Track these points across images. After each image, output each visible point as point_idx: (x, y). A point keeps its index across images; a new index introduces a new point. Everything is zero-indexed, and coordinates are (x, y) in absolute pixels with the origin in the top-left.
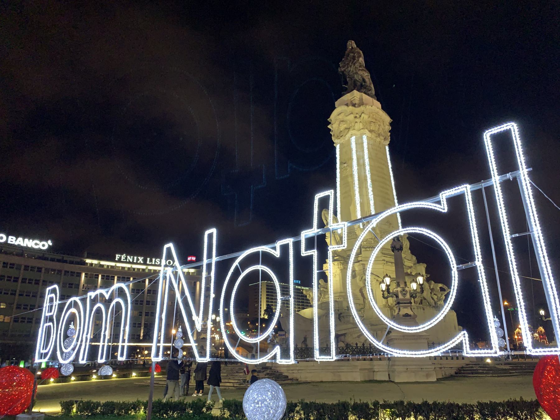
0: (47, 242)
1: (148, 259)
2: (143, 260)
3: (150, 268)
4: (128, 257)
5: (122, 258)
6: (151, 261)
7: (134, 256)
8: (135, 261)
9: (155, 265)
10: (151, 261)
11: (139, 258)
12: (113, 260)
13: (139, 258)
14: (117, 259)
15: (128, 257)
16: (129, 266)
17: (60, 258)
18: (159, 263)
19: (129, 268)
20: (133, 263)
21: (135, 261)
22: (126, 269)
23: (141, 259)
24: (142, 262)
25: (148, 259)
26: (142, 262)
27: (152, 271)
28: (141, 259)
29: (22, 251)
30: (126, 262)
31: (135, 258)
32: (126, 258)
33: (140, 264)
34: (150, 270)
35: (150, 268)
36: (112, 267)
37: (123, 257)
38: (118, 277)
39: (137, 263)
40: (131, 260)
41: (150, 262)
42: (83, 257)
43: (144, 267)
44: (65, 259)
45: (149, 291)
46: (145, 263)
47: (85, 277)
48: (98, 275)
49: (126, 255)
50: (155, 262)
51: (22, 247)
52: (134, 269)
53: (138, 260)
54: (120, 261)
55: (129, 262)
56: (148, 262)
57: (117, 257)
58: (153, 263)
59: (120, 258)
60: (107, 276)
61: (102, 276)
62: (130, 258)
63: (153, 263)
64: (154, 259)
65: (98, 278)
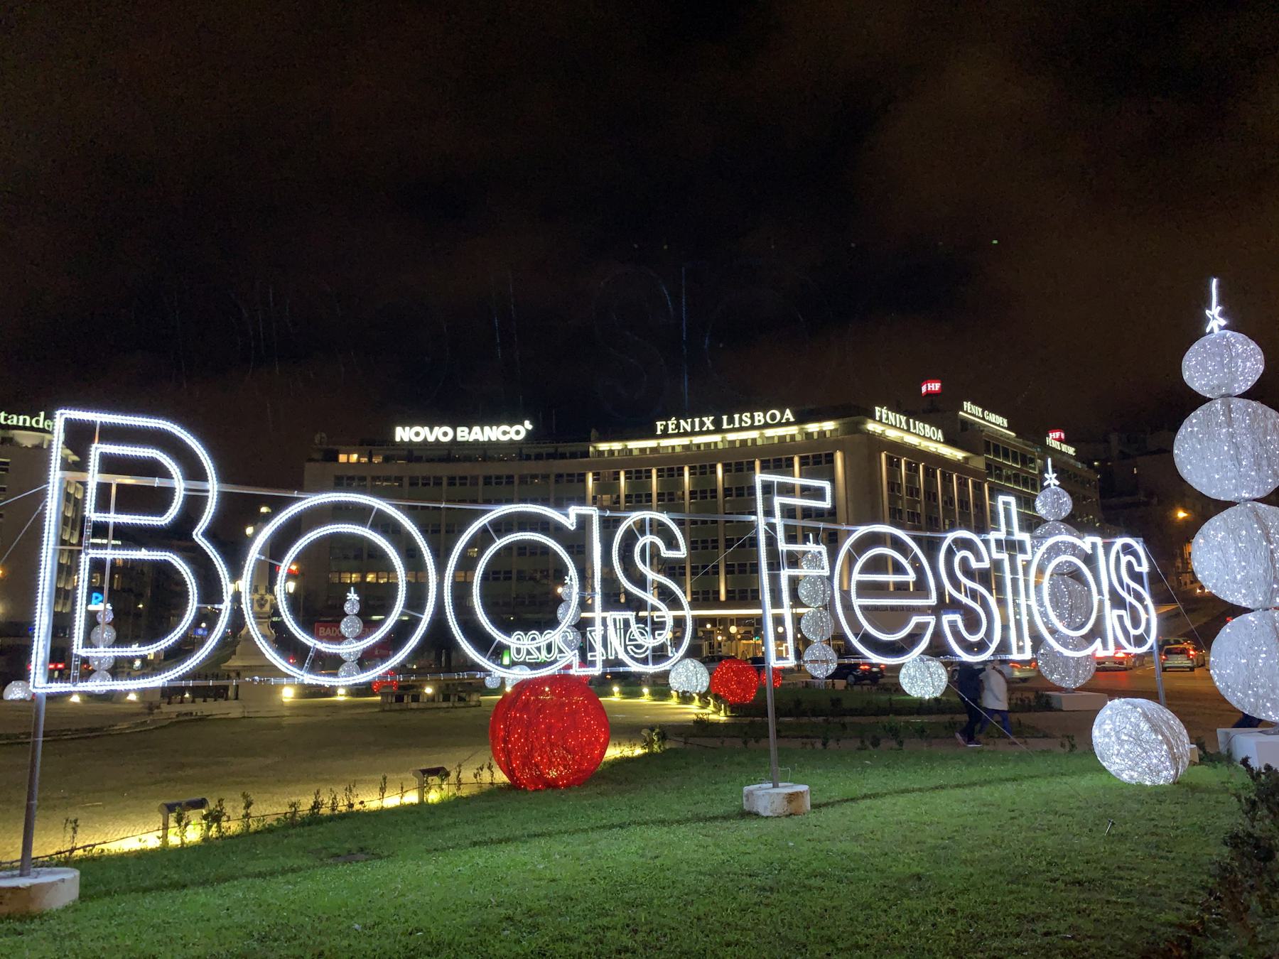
0: (523, 424)
1: (725, 418)
2: (713, 423)
3: (731, 437)
4: (682, 422)
5: (671, 427)
6: (731, 421)
7: (693, 417)
8: (697, 429)
9: (741, 429)
10: (731, 421)
11: (705, 419)
12: (652, 435)
13: (705, 419)
14: (659, 432)
15: (682, 422)
16: (685, 441)
17: (552, 450)
18: (749, 422)
19: (684, 446)
20: (693, 433)
21: (697, 429)
22: (636, 453)
23: (708, 421)
24: (712, 428)
25: (725, 418)
26: (712, 428)
27: (738, 445)
28: (708, 421)
29: (486, 451)
30: (679, 435)
31: (697, 420)
32: (678, 426)
33: (708, 432)
34: (734, 442)
35: (731, 437)
36: (653, 450)
37: (672, 424)
38: (658, 471)
39: (701, 433)
40: (689, 429)
41: (729, 423)
42: (588, 440)
43: (716, 438)
44: (560, 450)
45: (727, 491)
46: (718, 429)
47: (626, 478)
48: (618, 473)
49: (677, 420)
50: (741, 420)
51: (484, 443)
52: (698, 446)
53: (702, 424)
54: (665, 435)
55: (686, 434)
56: (725, 426)
57: (660, 425)
58: (737, 425)
59: (666, 427)
60: (637, 472)
61: (626, 473)
62: (685, 425)
63: (737, 425)
64: (737, 416)
65: (618, 479)
